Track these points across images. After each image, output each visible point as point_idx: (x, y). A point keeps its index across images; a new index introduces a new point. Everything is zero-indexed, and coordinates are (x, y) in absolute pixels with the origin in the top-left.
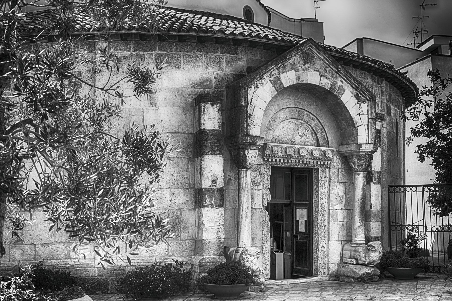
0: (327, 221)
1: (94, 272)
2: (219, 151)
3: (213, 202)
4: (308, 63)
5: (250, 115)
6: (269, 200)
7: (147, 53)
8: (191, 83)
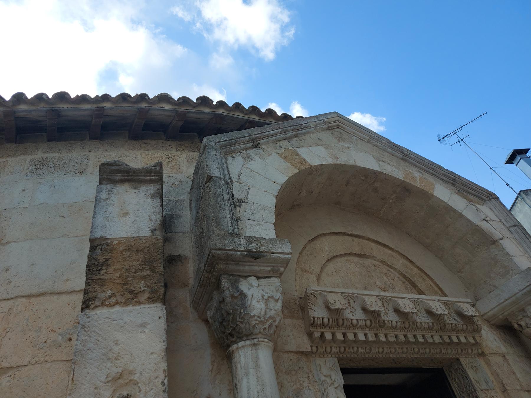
2: (153, 292)
4: (344, 141)
5: (241, 201)
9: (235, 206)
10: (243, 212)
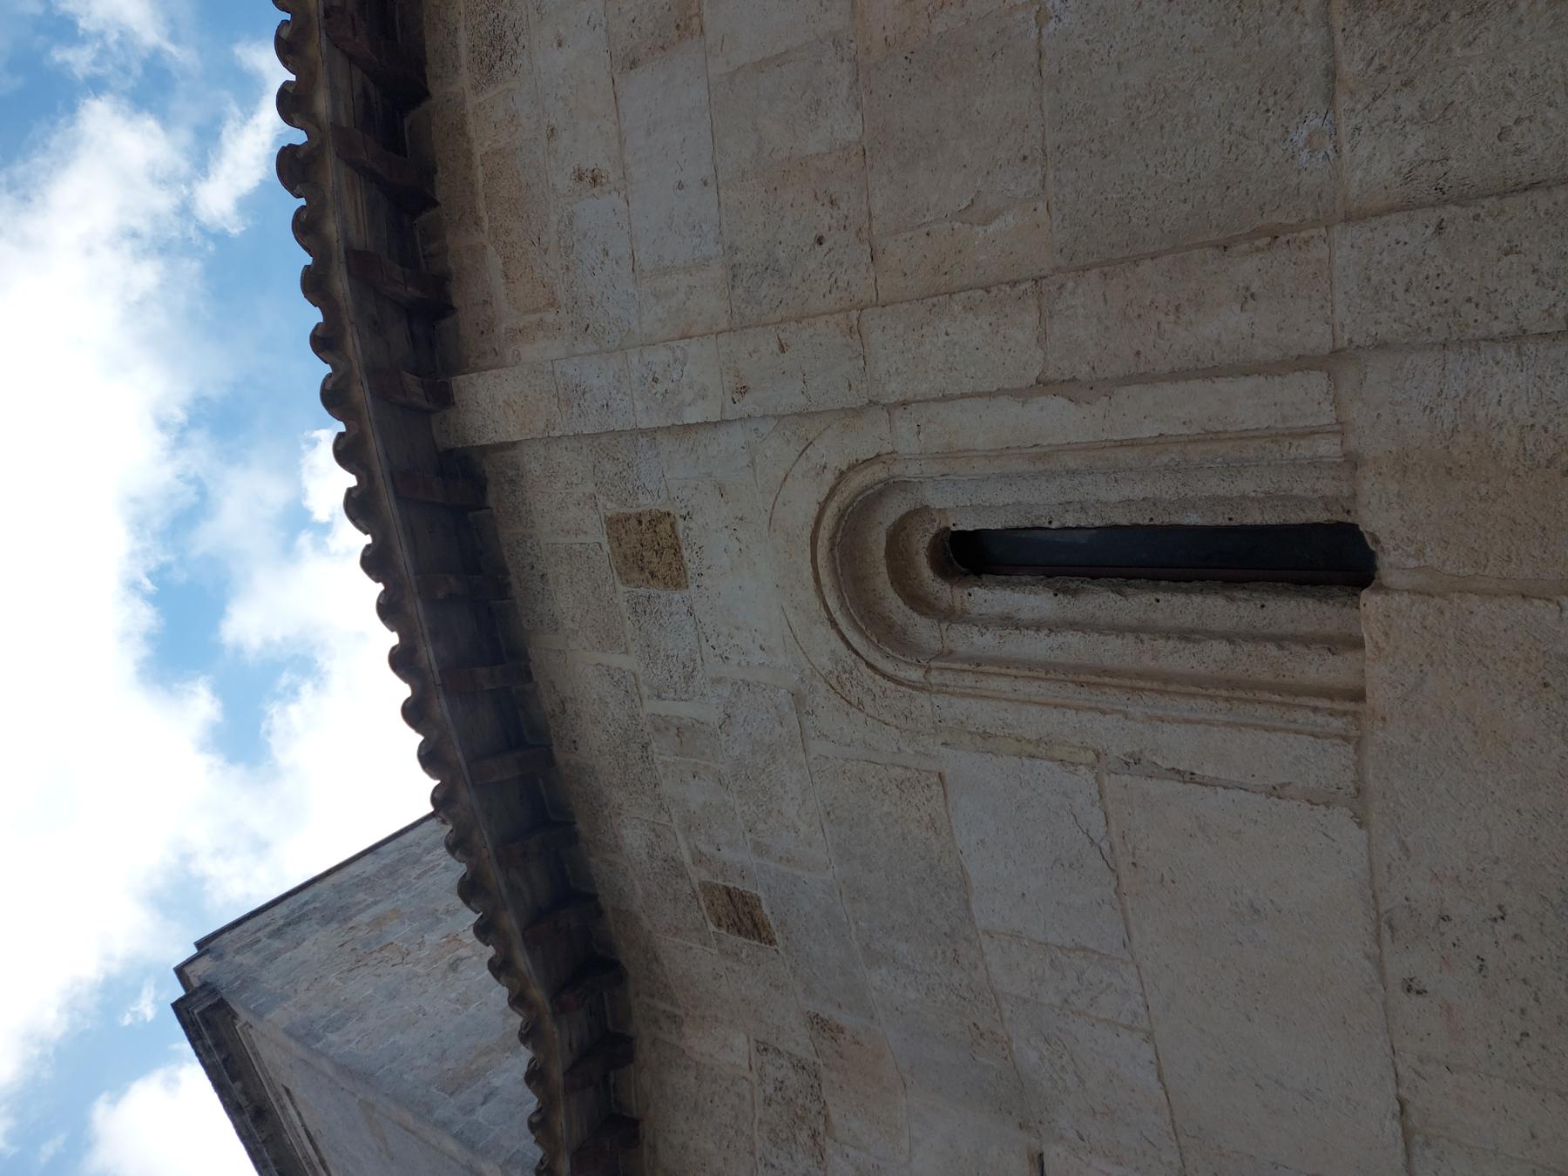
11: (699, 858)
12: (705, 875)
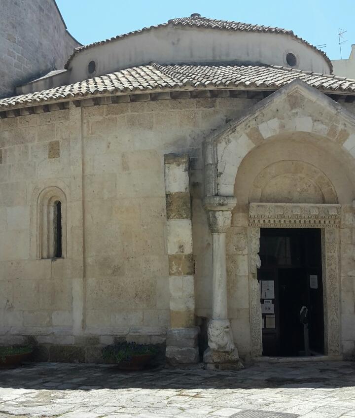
0: (338, 289)
1: (69, 341)
3: (180, 269)
4: (296, 108)
5: (221, 173)
6: (259, 265)
7: (119, 115)
8: (164, 143)
9: (218, 177)
10: (221, 180)
11: (6, 151)
12: (3, 152)
